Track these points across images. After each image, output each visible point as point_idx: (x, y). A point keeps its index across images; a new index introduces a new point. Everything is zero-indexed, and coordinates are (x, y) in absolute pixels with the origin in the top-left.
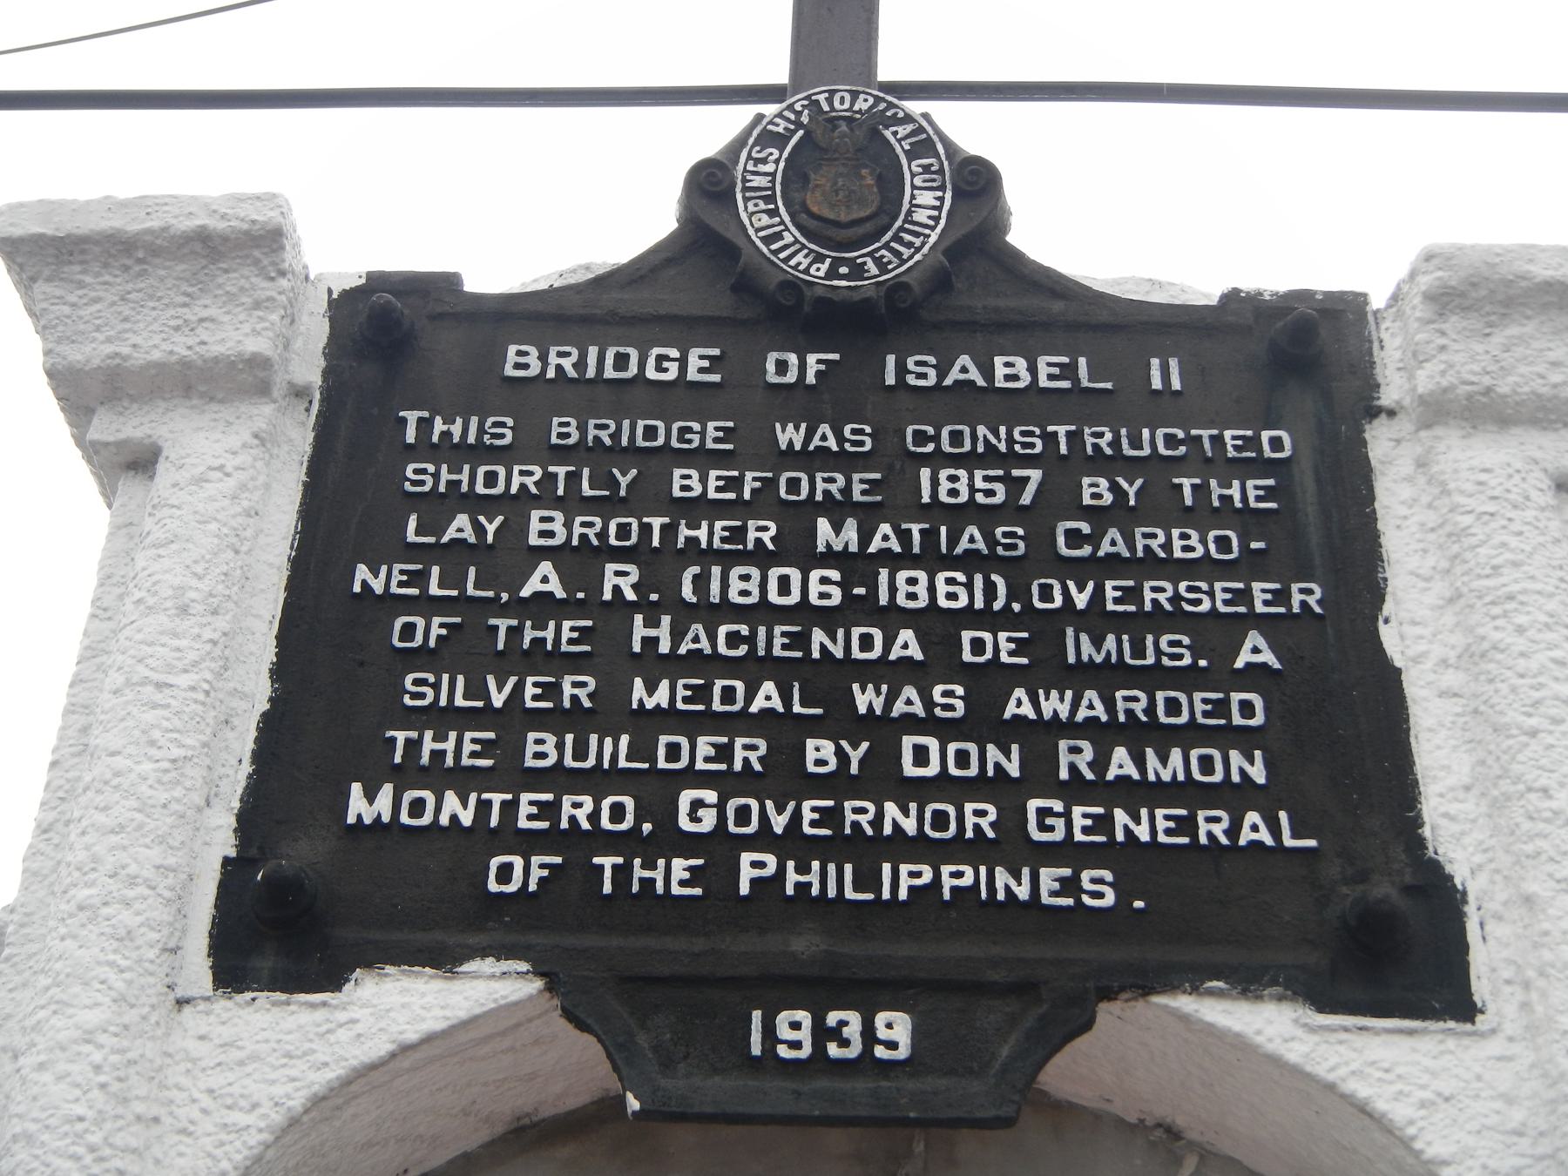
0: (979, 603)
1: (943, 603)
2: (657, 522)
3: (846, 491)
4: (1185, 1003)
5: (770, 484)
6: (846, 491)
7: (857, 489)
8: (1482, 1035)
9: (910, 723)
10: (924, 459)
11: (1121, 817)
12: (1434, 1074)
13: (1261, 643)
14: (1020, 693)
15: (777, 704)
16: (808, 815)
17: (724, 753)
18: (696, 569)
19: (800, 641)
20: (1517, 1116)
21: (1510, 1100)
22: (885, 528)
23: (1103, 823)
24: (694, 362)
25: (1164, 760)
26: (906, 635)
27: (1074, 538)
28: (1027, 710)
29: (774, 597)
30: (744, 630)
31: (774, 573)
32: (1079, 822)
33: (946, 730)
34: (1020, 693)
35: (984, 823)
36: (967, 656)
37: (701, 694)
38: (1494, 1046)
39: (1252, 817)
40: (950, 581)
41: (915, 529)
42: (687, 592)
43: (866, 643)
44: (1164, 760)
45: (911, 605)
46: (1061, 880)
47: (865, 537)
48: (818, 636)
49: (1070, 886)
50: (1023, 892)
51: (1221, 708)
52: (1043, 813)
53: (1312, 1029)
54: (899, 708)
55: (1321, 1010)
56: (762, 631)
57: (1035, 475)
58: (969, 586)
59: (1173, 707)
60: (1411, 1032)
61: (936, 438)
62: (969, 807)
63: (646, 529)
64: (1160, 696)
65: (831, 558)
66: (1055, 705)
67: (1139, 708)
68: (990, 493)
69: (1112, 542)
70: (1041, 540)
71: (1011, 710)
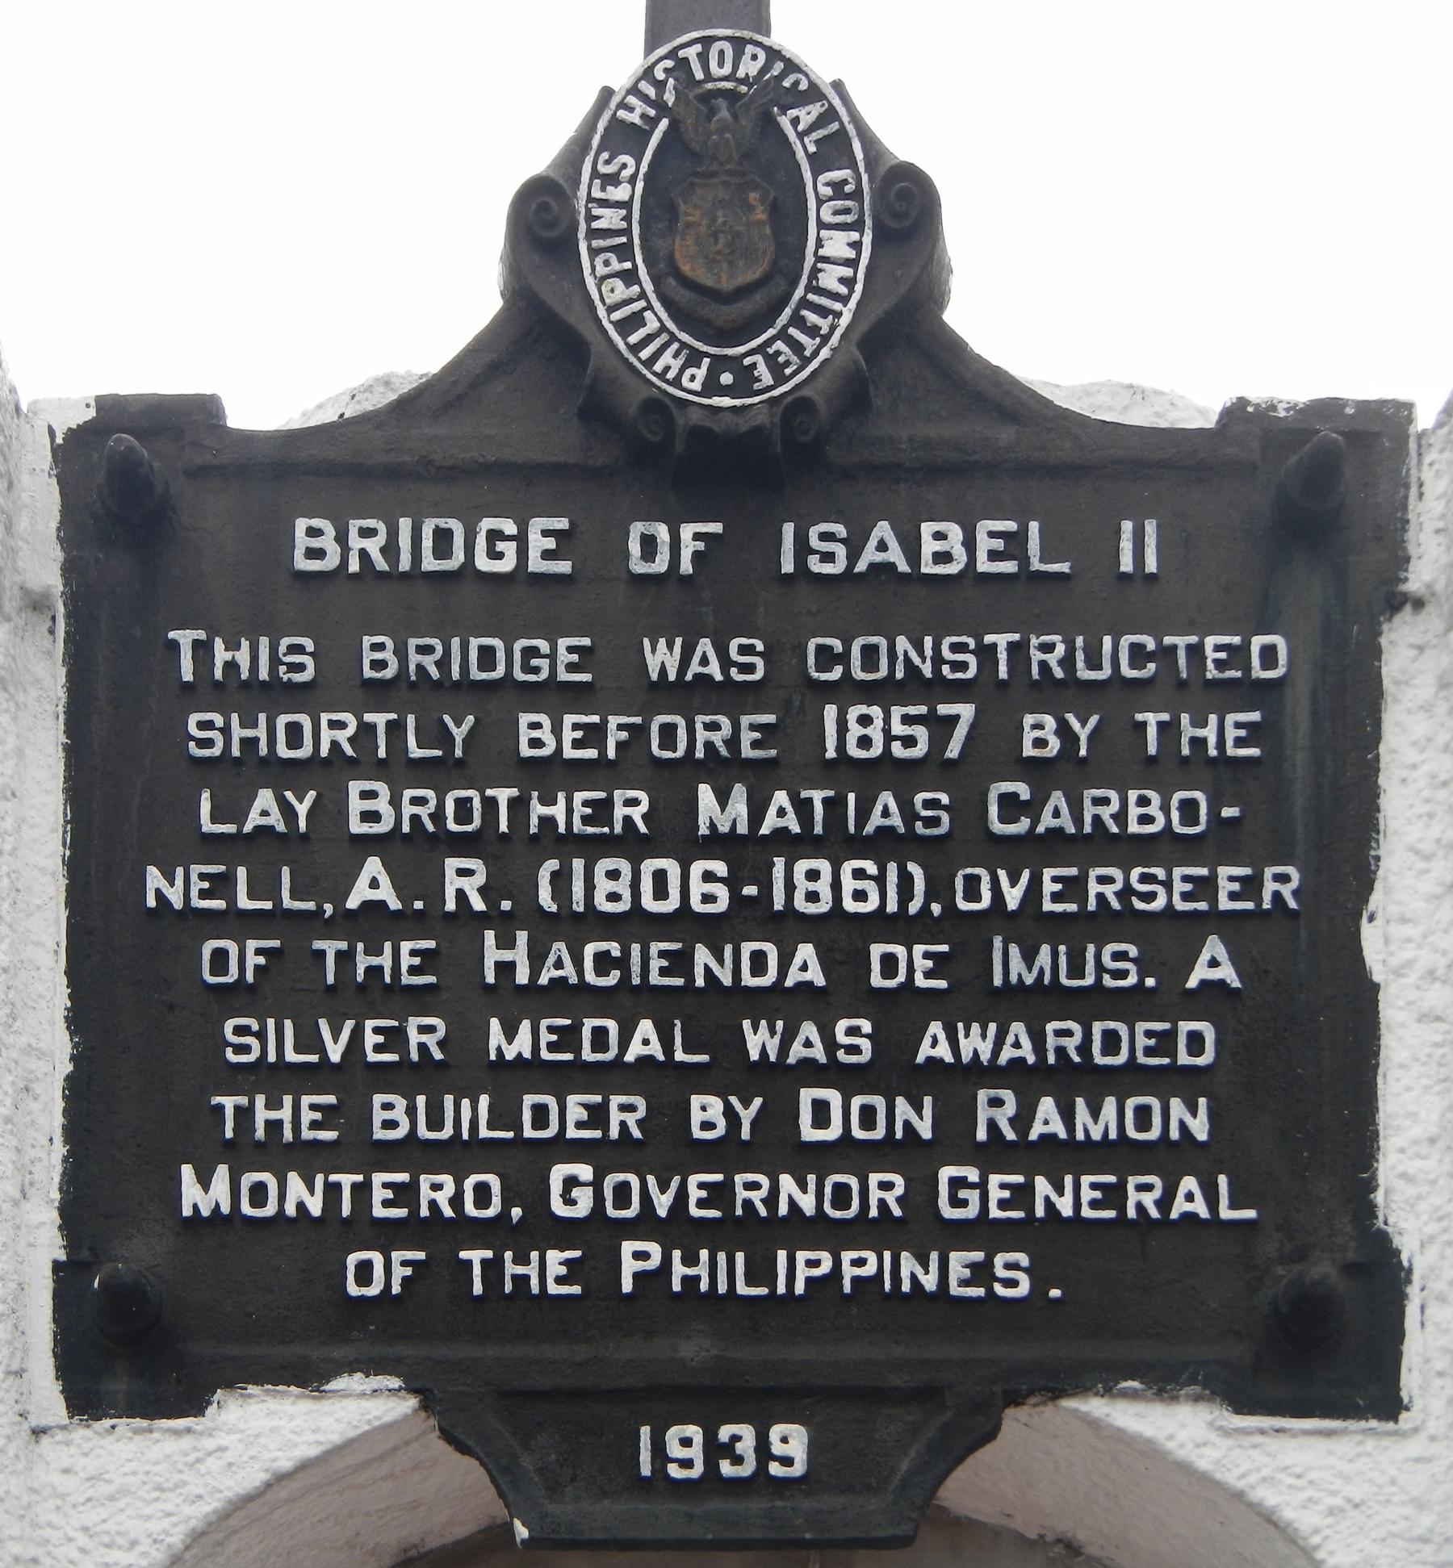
0: (892, 907)
1: (850, 905)
2: (503, 795)
3: (733, 742)
4: (1095, 1406)
5: (638, 733)
6: (733, 742)
7: (747, 737)
8: (1402, 1435)
9: (811, 1072)
10: (828, 691)
11: (1042, 1186)
12: (1347, 1479)
13: (1222, 953)
14: (936, 1028)
15: (656, 1050)
16: (695, 1194)
17: (597, 1116)
18: (552, 865)
19: (680, 962)
20: (1426, 1520)
21: (1420, 1504)
22: (781, 798)
23: (1022, 1195)
24: (538, 543)
25: (1095, 1113)
26: (806, 952)
27: (1011, 806)
28: (943, 1052)
29: (649, 903)
30: (615, 949)
31: (649, 866)
32: (996, 1194)
33: (848, 1079)
34: (936, 1028)
35: (890, 1198)
36: (876, 980)
37: (568, 1038)
38: (1414, 1447)
39: (1189, 1183)
40: (859, 874)
41: (817, 796)
42: (545, 898)
43: (759, 963)
44: (1095, 1113)
45: (812, 909)
46: (972, 1266)
47: (757, 814)
48: (702, 956)
49: (981, 1273)
50: (930, 1282)
51: (1165, 1043)
52: (957, 1183)
53: (1226, 1433)
54: (797, 1052)
55: (1238, 1411)
56: (636, 949)
57: (966, 711)
58: (881, 880)
59: (1111, 1042)
60: (1329, 1434)
61: (844, 658)
62: (874, 1179)
63: (490, 804)
64: (1097, 1028)
65: (718, 843)
66: (976, 1043)
67: (1071, 1044)
68: (909, 742)
69: (1055, 814)
70: (969, 810)
71: (925, 1052)
